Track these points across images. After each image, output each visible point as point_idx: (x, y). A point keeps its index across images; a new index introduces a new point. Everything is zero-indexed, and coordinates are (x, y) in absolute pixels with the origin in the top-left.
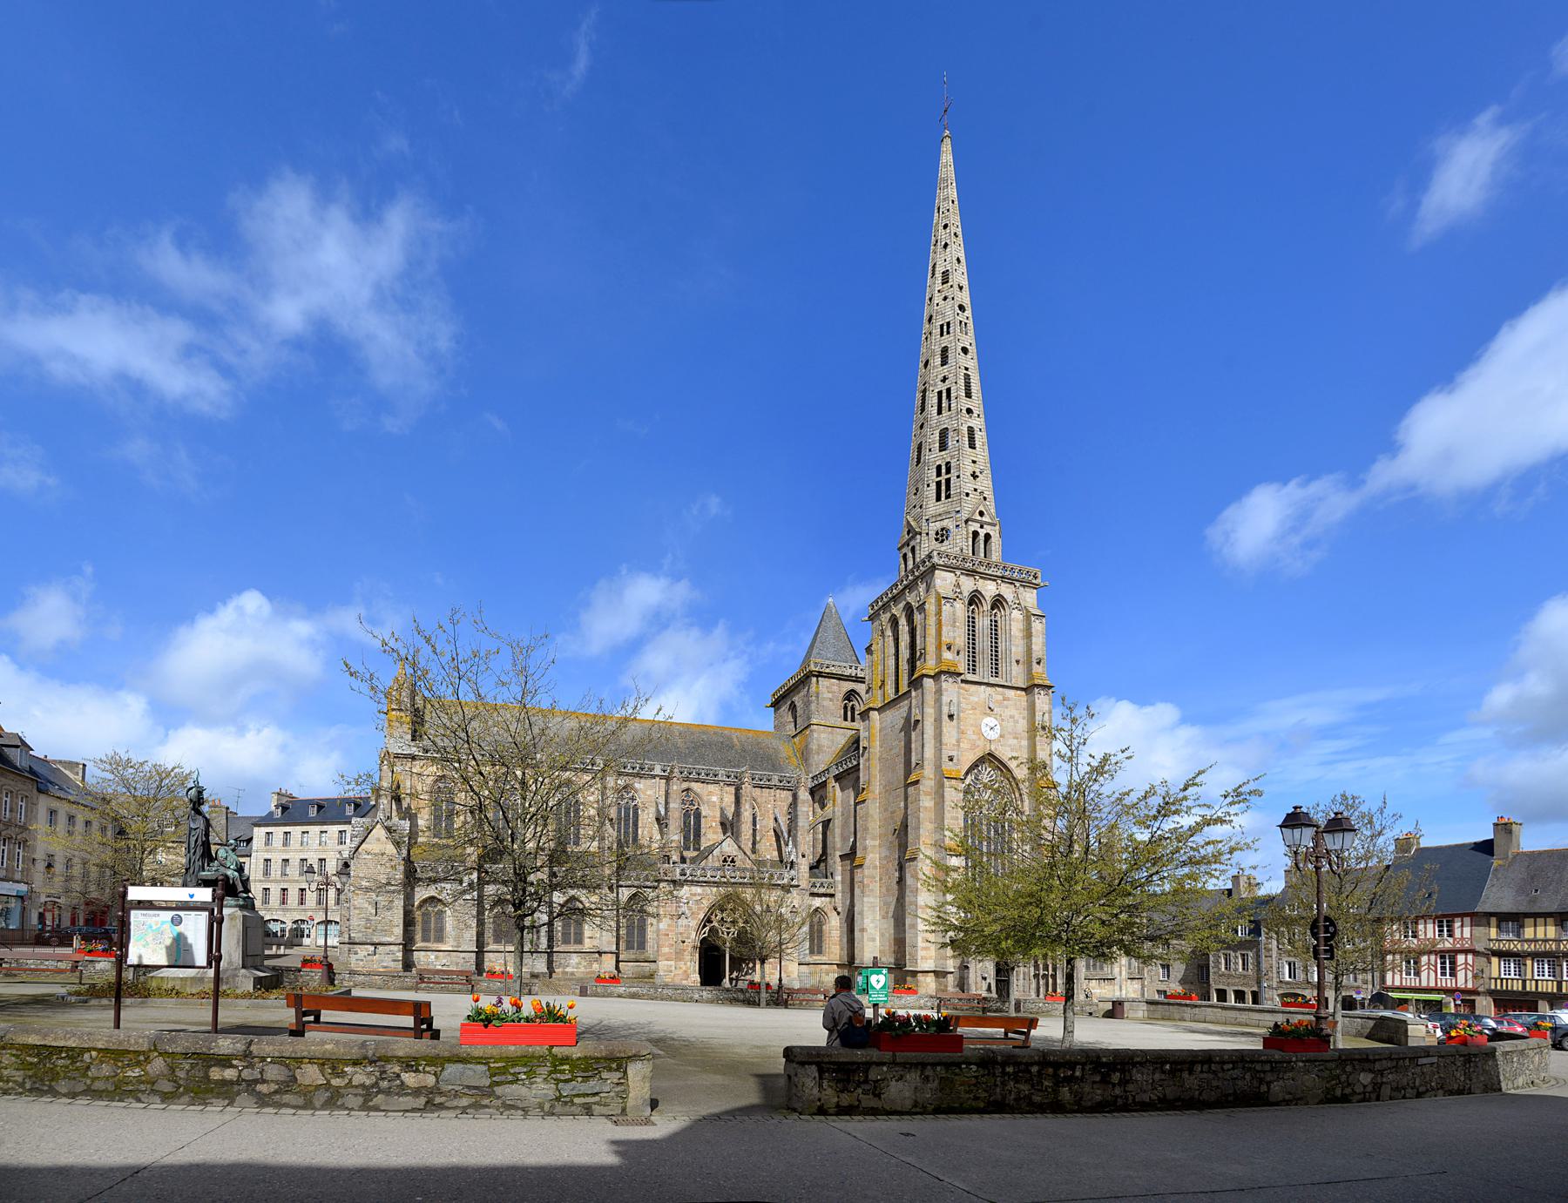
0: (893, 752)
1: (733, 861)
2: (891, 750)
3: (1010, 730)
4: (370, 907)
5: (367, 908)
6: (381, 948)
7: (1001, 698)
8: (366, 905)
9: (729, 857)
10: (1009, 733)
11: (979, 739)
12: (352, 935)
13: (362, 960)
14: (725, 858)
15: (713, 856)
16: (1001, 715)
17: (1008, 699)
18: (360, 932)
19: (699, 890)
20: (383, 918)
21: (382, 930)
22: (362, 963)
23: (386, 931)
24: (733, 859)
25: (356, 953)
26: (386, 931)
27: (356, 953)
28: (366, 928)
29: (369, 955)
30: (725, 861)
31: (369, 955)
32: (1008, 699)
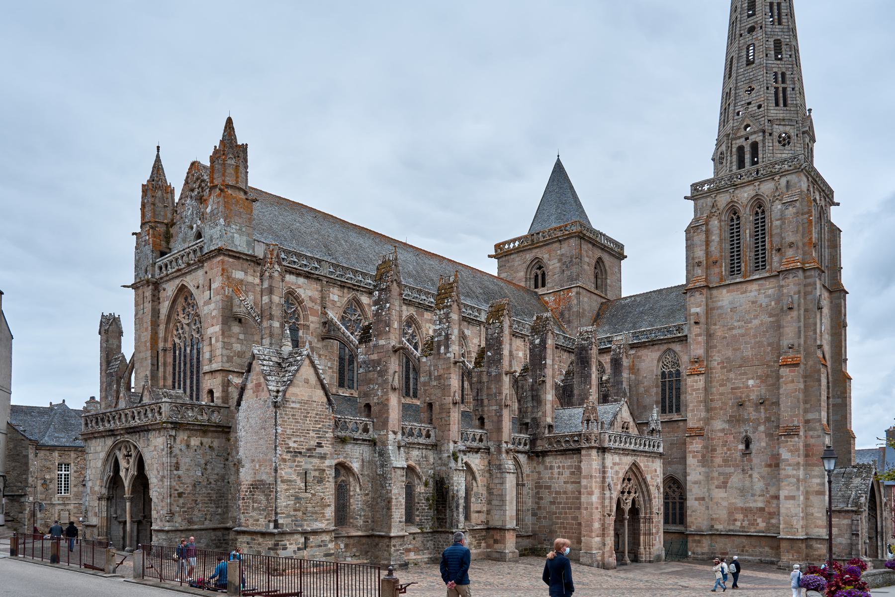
0: (735, 332)
2: (730, 329)
4: (299, 482)
5: (295, 481)
8: (294, 477)
12: (280, 521)
18: (288, 516)
19: (617, 458)
20: (313, 495)
21: (313, 513)
25: (285, 549)
26: (316, 513)
27: (285, 549)
28: (295, 510)
29: (299, 549)
30: (623, 428)
31: (299, 549)
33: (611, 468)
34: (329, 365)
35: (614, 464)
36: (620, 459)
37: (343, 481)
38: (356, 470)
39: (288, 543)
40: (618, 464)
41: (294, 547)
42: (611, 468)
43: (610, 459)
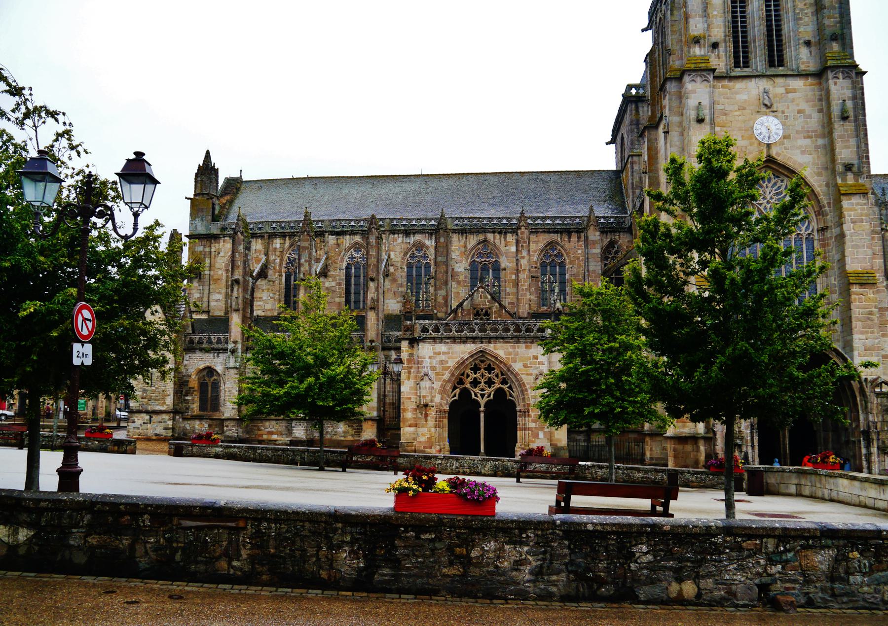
1: (487, 314)
3: (799, 128)
6: (154, 417)
7: (781, 90)
9: (482, 310)
10: (798, 132)
11: (751, 144)
13: (138, 428)
14: (478, 312)
15: (463, 309)
16: (783, 112)
17: (794, 91)
19: (442, 348)
21: (156, 400)
22: (138, 431)
23: (158, 400)
24: (486, 312)
25: (134, 422)
26: (158, 400)
27: (134, 422)
29: (144, 423)
31: (144, 423)
32: (794, 91)
33: (430, 358)
34: (271, 295)
35: (439, 353)
36: (449, 349)
37: (215, 380)
38: (219, 371)
39: (136, 419)
40: (444, 353)
41: (141, 422)
42: (430, 358)
43: (425, 350)
